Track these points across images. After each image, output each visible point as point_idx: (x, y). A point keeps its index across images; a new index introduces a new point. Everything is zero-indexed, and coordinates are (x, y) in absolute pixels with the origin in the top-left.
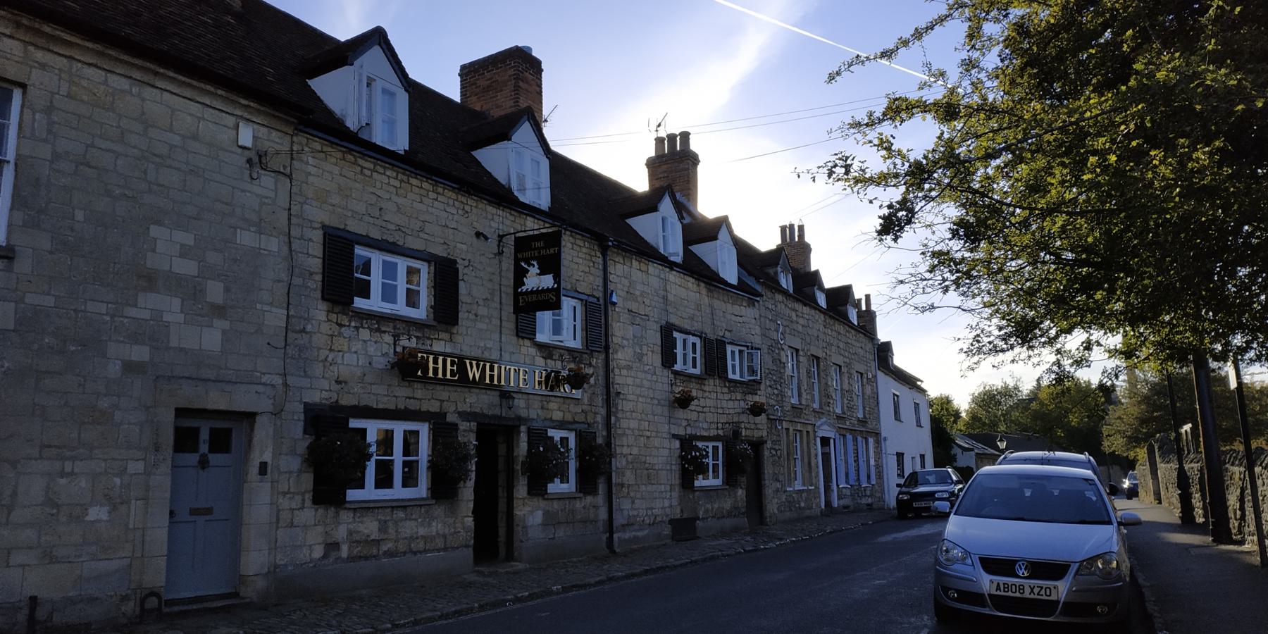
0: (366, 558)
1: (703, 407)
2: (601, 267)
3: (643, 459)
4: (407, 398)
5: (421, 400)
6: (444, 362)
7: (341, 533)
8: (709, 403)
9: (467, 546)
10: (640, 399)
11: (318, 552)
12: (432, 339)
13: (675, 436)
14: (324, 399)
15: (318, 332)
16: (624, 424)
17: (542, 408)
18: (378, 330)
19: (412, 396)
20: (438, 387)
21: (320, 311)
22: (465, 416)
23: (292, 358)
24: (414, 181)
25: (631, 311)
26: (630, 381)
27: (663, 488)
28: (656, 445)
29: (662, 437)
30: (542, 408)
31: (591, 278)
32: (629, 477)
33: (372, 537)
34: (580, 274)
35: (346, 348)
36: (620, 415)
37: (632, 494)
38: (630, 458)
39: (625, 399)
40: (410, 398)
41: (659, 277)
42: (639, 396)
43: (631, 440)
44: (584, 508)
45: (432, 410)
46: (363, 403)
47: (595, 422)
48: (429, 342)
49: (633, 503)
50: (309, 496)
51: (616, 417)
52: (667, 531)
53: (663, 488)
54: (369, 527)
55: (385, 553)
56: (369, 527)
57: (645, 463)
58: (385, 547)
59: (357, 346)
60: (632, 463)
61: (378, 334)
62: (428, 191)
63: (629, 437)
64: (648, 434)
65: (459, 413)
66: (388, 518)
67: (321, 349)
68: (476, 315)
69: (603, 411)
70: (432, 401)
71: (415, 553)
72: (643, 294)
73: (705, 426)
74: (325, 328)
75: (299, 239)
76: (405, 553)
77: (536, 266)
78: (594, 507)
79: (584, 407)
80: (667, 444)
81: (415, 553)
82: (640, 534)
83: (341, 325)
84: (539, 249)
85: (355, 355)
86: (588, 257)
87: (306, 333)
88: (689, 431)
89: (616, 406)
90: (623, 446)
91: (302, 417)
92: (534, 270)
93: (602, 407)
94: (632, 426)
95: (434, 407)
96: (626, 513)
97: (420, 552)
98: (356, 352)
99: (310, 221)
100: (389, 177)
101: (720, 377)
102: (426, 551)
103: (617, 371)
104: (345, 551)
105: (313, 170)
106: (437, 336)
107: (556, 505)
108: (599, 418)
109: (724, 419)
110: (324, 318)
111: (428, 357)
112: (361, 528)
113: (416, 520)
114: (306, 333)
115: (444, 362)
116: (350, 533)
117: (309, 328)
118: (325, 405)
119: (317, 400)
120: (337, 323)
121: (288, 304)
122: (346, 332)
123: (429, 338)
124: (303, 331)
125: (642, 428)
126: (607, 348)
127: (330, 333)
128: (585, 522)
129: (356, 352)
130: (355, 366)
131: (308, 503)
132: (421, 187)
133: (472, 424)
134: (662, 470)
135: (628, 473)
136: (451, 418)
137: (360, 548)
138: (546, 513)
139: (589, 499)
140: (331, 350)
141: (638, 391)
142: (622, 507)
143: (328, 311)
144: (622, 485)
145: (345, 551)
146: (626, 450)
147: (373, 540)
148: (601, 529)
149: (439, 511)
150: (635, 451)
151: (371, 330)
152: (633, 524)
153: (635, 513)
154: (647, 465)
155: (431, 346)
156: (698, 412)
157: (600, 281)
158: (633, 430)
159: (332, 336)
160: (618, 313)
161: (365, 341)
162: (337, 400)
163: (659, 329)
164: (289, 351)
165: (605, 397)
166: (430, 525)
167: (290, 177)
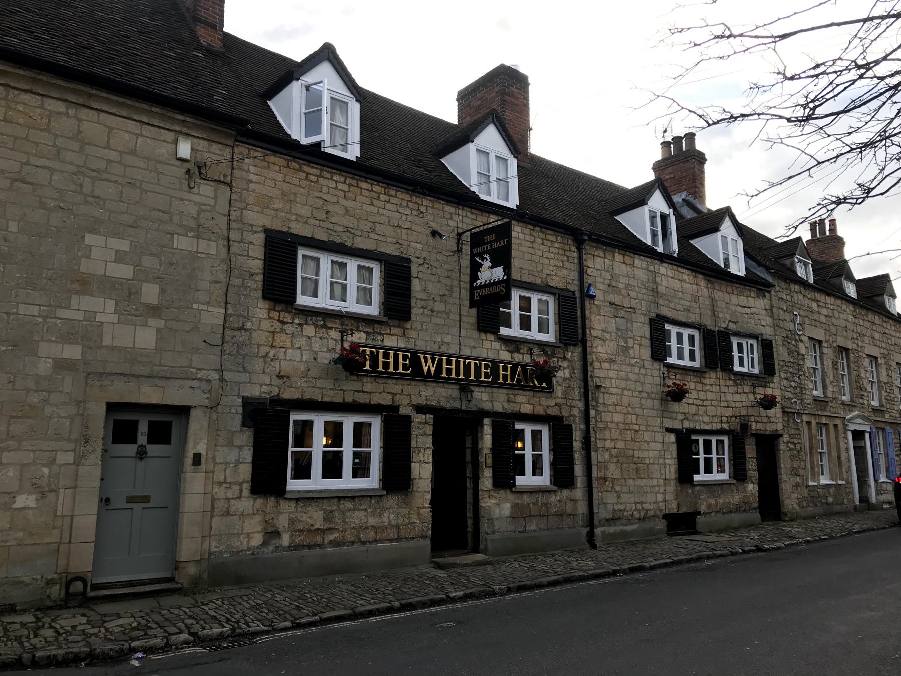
0: (310, 547)
1: (703, 400)
2: (576, 261)
3: (631, 452)
4: (355, 391)
5: (371, 393)
6: (396, 357)
7: (282, 522)
8: (710, 396)
9: (424, 537)
10: (626, 392)
11: (257, 540)
12: (383, 335)
13: (670, 430)
14: (264, 392)
15: (259, 329)
16: (606, 417)
17: (508, 401)
18: (325, 327)
19: (361, 389)
20: (390, 381)
21: (260, 310)
22: (421, 409)
23: (229, 354)
24: (364, 185)
25: (614, 304)
26: (612, 374)
27: (655, 482)
28: (646, 439)
29: (653, 431)
30: (508, 401)
31: (564, 272)
32: (613, 471)
33: (316, 527)
34: (551, 268)
35: (288, 344)
36: (601, 408)
37: (617, 488)
38: (614, 452)
39: (607, 392)
40: (359, 391)
41: (647, 269)
42: (623, 389)
43: (615, 434)
44: (559, 501)
45: (383, 402)
46: (307, 396)
47: (571, 415)
48: (379, 337)
49: (619, 497)
50: (246, 487)
51: (597, 410)
52: (661, 525)
53: (655, 482)
54: (315, 517)
55: (331, 542)
56: (315, 517)
57: (633, 456)
59: (301, 342)
60: (616, 457)
61: (324, 330)
62: (380, 194)
63: (613, 431)
64: (636, 427)
65: (413, 405)
66: (335, 508)
67: (261, 345)
68: (432, 311)
69: (581, 405)
70: (385, 395)
71: (364, 543)
72: (627, 286)
73: (706, 419)
74: (266, 325)
75: (239, 243)
76: (353, 543)
77: (489, 260)
78: (571, 500)
79: (559, 401)
80: (659, 437)
81: (364, 543)
82: (628, 528)
83: (283, 323)
84: (491, 242)
85: (299, 351)
86: (561, 252)
87: (246, 330)
88: (687, 424)
89: (596, 399)
90: (605, 440)
91: (240, 410)
92: (487, 264)
93: (579, 400)
94: (615, 419)
95: (386, 400)
96: (610, 507)
97: (371, 542)
98: (299, 348)
99: (251, 225)
100: (336, 181)
101: (723, 370)
102: (376, 541)
103: (596, 364)
104: (286, 540)
105: (254, 178)
106: (389, 332)
107: (526, 499)
108: (576, 412)
109: (729, 412)
110: (266, 316)
111: (378, 352)
112: (305, 517)
113: (365, 510)
114: (246, 330)
115: (396, 357)
116: (292, 521)
117: (248, 325)
118: (266, 398)
119: (257, 394)
120: (279, 321)
121: (226, 303)
122: (290, 329)
123: (380, 334)
124: (242, 328)
125: (628, 421)
126: (584, 342)
127: (271, 330)
128: (561, 515)
129: (299, 348)
130: (298, 362)
131: (246, 492)
132: (372, 190)
133: (429, 416)
134: (654, 463)
135: (612, 467)
136: (403, 411)
137: (302, 537)
138: (515, 506)
139: (565, 493)
140: (272, 346)
141: (623, 384)
142: (605, 501)
143: (269, 310)
144: (605, 479)
145: (286, 540)
146: (608, 444)
147: (316, 529)
148: (580, 523)
149: (392, 501)
150: (620, 445)
151: (316, 326)
152: (619, 518)
153: (622, 507)
154: (635, 459)
155: (383, 341)
156: (698, 406)
157: (575, 275)
158: (617, 423)
159: (273, 333)
160: (597, 306)
161: (309, 337)
162: (278, 394)
163: (647, 322)
164: (227, 347)
165: (582, 390)
166: (381, 515)
167: (230, 185)
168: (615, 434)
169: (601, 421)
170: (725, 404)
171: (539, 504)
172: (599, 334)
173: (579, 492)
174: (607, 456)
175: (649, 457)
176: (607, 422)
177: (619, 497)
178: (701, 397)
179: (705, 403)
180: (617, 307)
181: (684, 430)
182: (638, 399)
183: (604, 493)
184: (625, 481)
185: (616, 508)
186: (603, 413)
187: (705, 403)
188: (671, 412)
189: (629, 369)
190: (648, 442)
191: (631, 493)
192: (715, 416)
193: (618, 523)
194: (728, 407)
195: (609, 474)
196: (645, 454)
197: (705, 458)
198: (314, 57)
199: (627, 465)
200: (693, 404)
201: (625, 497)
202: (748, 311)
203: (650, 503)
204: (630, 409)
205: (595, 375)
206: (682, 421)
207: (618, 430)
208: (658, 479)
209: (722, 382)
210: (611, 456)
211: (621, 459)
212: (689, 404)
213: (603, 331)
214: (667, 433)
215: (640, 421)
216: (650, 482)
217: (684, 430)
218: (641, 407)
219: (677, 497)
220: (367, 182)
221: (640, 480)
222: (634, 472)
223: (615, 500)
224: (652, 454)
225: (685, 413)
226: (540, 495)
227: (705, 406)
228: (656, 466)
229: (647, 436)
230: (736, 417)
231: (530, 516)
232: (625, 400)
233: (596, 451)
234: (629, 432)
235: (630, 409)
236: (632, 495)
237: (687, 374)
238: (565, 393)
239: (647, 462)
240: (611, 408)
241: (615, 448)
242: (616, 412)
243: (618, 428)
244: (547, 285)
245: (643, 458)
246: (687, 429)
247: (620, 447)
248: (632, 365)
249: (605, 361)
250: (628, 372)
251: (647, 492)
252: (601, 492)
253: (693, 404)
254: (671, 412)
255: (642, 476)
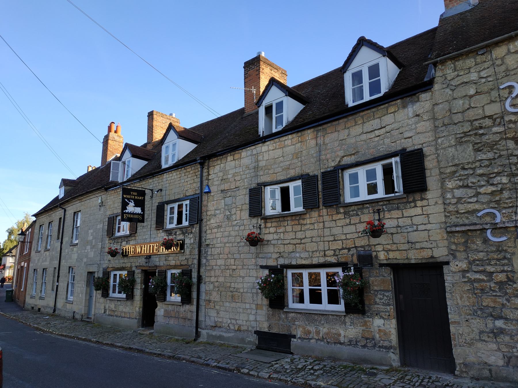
1: (301, 239)
3: (229, 284)
8: (309, 234)
9: (136, 319)
10: (227, 245)
13: (262, 267)
16: (212, 263)
17: (166, 260)
25: (224, 190)
26: (219, 235)
27: (248, 306)
28: (242, 275)
29: (248, 269)
32: (215, 296)
36: (209, 258)
37: (217, 307)
38: (216, 284)
41: (251, 155)
42: (225, 243)
43: (218, 273)
49: (218, 313)
52: (254, 339)
53: (248, 306)
54: (112, 306)
55: (115, 315)
56: (112, 306)
57: (230, 287)
58: (116, 313)
60: (218, 287)
63: (217, 271)
64: (235, 267)
68: (143, 226)
71: (122, 317)
72: (234, 175)
73: (306, 255)
77: (133, 203)
78: (190, 311)
79: (187, 257)
80: (253, 273)
81: (122, 317)
82: (225, 335)
84: (135, 196)
86: (194, 174)
88: (281, 261)
89: (206, 252)
90: (211, 277)
92: (132, 204)
94: (219, 264)
96: (212, 318)
101: (327, 205)
102: (124, 317)
103: (209, 232)
107: (170, 308)
109: (338, 245)
116: (109, 307)
125: (228, 264)
128: (185, 319)
134: (247, 292)
135: (214, 294)
136: (134, 269)
138: (166, 311)
141: (226, 240)
142: (209, 315)
144: (210, 301)
146: (213, 279)
149: (129, 303)
150: (221, 279)
152: (220, 327)
153: (220, 320)
154: (231, 289)
156: (295, 244)
158: (220, 266)
163: (248, 192)
168: (218, 273)
169: (209, 265)
170: (332, 238)
171: (175, 311)
172: (213, 213)
173: (194, 308)
174: (211, 286)
175: (243, 288)
176: (213, 266)
177: (218, 313)
178: (300, 237)
179: (303, 241)
180: (226, 191)
181: (279, 267)
182: (236, 248)
183: (209, 310)
184: (223, 304)
185: (216, 320)
186: (210, 261)
187: (303, 241)
188: (266, 253)
189: (231, 229)
190: (243, 277)
191: (227, 312)
192: (316, 251)
193: (220, 330)
194: (335, 240)
195: (212, 298)
196: (240, 286)
197: (310, 290)
198: (356, 47)
199: (225, 293)
200: (290, 244)
201: (222, 314)
202: (383, 130)
203: (243, 321)
204: (230, 256)
205: (207, 238)
206: (277, 259)
207: (220, 270)
208: (250, 304)
209: (326, 218)
210: (214, 287)
211: (221, 289)
212: (284, 244)
213: (215, 210)
214: (261, 270)
215: (237, 262)
216: (243, 306)
217: (279, 267)
218: (238, 253)
219: (269, 319)
220: (392, 105)
221: (234, 303)
222: (230, 298)
223: (215, 315)
224: (245, 285)
225: (280, 253)
226: (176, 307)
227: (304, 243)
228: (249, 294)
229: (242, 273)
230: (349, 249)
231: (171, 317)
232: (226, 250)
233: (205, 283)
234: (228, 271)
235: (230, 256)
236: (228, 313)
237: (285, 221)
238: (191, 252)
239: (241, 291)
240: (216, 257)
241: (217, 281)
242: (220, 259)
243: (220, 269)
244: (186, 196)
245: (238, 289)
246: (281, 266)
247: (221, 281)
248: (234, 226)
249: (216, 227)
250: (230, 232)
251: (240, 313)
252: (207, 309)
253: (290, 244)
254: (266, 253)
255: (237, 301)
